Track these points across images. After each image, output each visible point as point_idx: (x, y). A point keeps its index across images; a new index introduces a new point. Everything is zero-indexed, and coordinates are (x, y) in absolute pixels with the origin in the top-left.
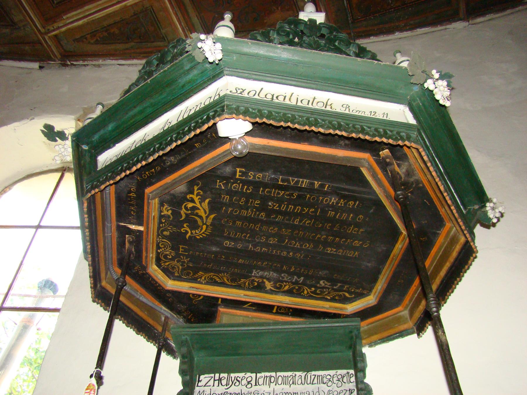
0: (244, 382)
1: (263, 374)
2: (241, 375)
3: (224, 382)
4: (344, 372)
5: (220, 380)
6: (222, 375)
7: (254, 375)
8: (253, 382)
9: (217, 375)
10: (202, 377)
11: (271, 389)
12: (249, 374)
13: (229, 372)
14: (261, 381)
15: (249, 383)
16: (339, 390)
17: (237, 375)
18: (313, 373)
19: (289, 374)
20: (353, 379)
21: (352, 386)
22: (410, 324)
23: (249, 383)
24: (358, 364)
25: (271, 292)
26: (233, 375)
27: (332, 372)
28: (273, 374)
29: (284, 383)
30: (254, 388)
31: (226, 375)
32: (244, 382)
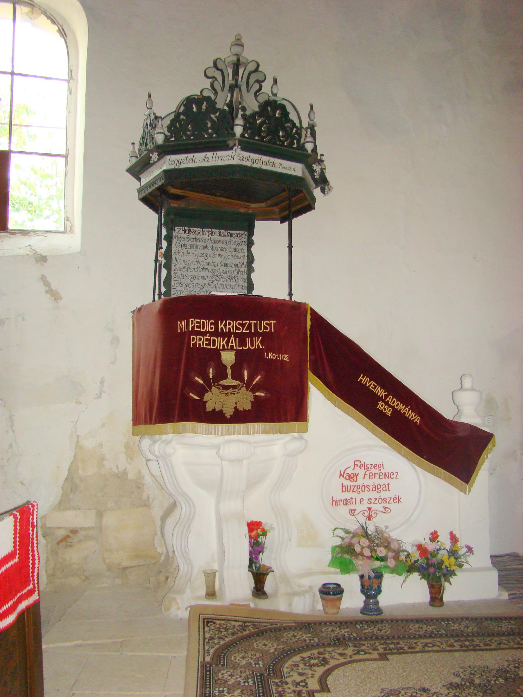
0: (197, 233)
1: (205, 230)
2: (195, 229)
3: (187, 232)
4: (243, 232)
5: (185, 230)
6: (186, 228)
7: (201, 230)
8: (201, 233)
9: (183, 228)
10: (176, 228)
11: (209, 237)
12: (199, 229)
13: (189, 227)
14: (205, 233)
15: (199, 233)
16: (240, 241)
17: (193, 229)
18: (229, 231)
19: (218, 230)
20: (246, 237)
21: (246, 240)
22: (278, 217)
23: (199, 233)
24: (250, 230)
25: (218, 196)
26: (191, 229)
27: (237, 232)
28: (210, 230)
29: (215, 235)
30: (201, 236)
31: (188, 228)
32: (197, 233)
